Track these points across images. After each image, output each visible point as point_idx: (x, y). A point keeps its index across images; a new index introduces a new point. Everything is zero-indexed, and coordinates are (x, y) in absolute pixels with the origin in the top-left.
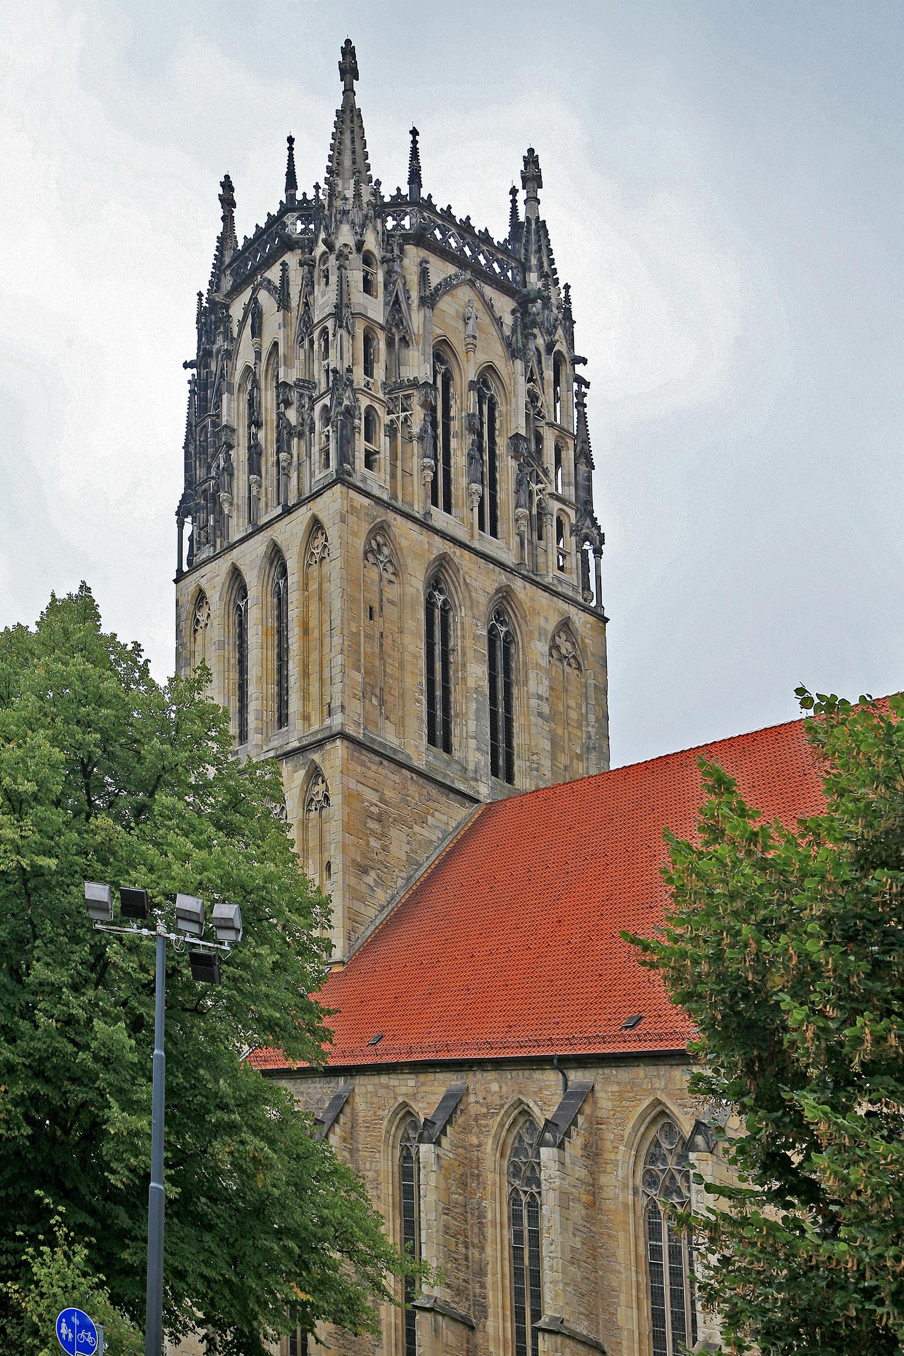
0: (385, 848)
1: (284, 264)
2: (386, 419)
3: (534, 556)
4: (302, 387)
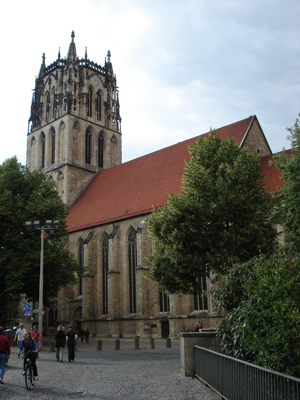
0: (76, 186)
1: (57, 71)
2: (79, 101)
3: (108, 124)
4: (60, 95)
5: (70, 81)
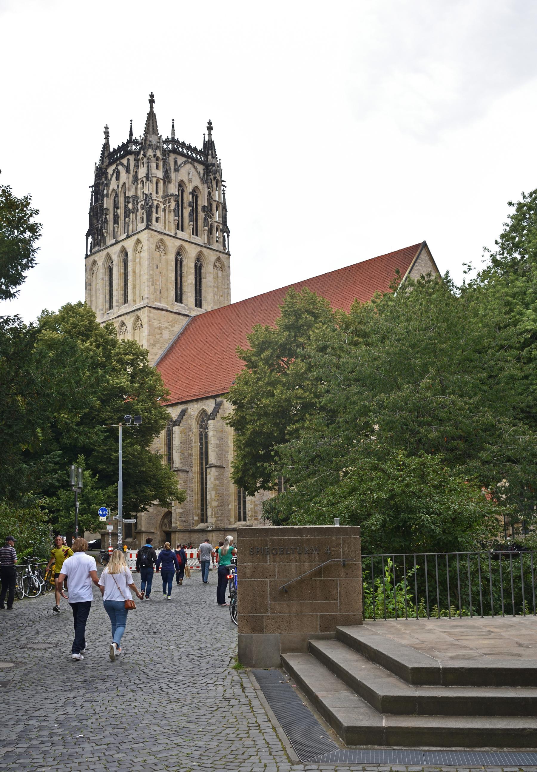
1: (128, 159)
5: (150, 175)
